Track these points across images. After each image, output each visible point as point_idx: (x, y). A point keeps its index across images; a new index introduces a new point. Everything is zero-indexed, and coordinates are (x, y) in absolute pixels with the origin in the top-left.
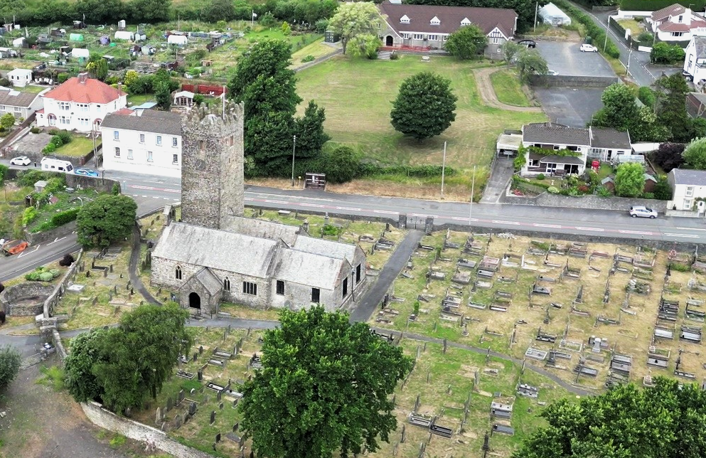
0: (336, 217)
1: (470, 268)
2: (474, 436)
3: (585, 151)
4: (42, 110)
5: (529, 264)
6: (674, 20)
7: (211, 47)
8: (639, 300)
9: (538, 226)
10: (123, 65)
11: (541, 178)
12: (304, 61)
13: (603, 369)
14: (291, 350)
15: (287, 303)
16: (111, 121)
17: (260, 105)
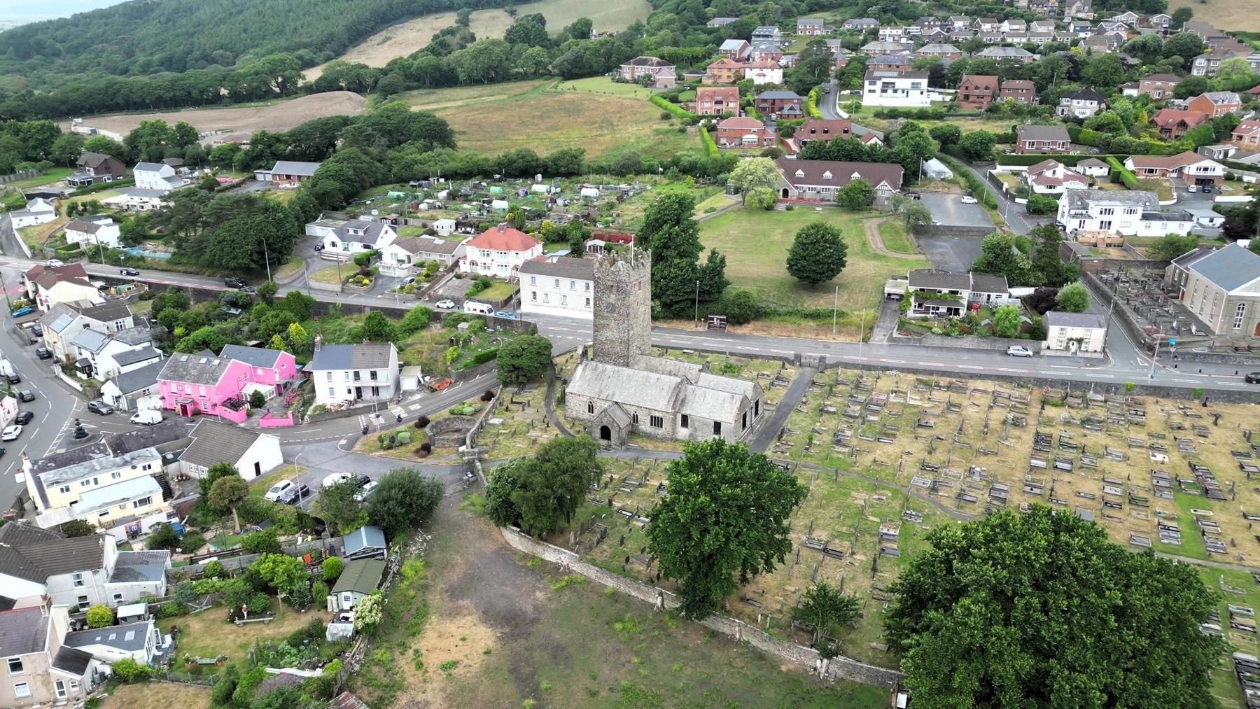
1: (860, 403)
2: (864, 558)
3: (966, 295)
4: (465, 257)
5: (914, 399)
6: (1049, 174)
7: (620, 199)
8: (1016, 432)
9: (923, 364)
10: (540, 215)
11: (926, 320)
13: (982, 497)
14: (694, 478)
15: (691, 435)
16: (528, 267)
17: (666, 253)
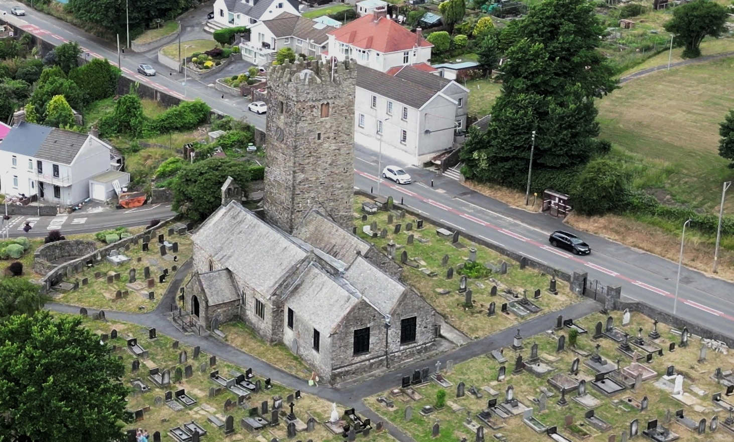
0: (508, 255)
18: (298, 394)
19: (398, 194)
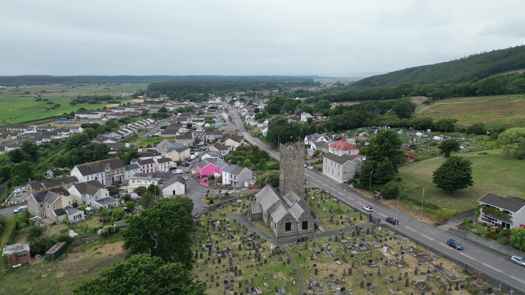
12: (480, 154)
18: (265, 241)
19: (332, 190)
